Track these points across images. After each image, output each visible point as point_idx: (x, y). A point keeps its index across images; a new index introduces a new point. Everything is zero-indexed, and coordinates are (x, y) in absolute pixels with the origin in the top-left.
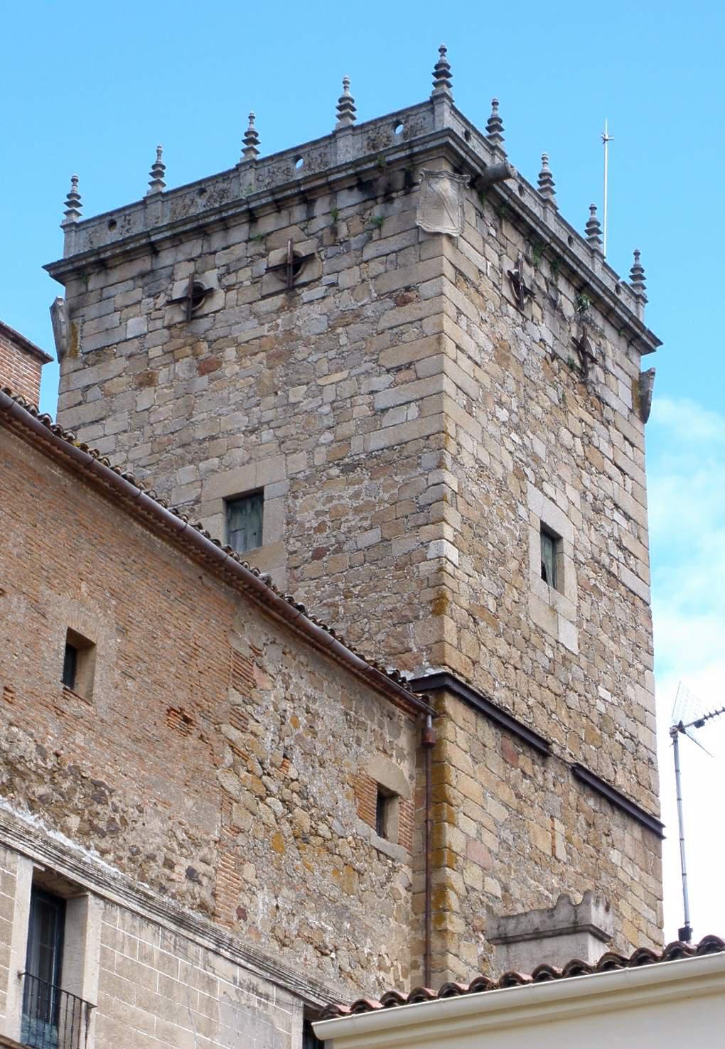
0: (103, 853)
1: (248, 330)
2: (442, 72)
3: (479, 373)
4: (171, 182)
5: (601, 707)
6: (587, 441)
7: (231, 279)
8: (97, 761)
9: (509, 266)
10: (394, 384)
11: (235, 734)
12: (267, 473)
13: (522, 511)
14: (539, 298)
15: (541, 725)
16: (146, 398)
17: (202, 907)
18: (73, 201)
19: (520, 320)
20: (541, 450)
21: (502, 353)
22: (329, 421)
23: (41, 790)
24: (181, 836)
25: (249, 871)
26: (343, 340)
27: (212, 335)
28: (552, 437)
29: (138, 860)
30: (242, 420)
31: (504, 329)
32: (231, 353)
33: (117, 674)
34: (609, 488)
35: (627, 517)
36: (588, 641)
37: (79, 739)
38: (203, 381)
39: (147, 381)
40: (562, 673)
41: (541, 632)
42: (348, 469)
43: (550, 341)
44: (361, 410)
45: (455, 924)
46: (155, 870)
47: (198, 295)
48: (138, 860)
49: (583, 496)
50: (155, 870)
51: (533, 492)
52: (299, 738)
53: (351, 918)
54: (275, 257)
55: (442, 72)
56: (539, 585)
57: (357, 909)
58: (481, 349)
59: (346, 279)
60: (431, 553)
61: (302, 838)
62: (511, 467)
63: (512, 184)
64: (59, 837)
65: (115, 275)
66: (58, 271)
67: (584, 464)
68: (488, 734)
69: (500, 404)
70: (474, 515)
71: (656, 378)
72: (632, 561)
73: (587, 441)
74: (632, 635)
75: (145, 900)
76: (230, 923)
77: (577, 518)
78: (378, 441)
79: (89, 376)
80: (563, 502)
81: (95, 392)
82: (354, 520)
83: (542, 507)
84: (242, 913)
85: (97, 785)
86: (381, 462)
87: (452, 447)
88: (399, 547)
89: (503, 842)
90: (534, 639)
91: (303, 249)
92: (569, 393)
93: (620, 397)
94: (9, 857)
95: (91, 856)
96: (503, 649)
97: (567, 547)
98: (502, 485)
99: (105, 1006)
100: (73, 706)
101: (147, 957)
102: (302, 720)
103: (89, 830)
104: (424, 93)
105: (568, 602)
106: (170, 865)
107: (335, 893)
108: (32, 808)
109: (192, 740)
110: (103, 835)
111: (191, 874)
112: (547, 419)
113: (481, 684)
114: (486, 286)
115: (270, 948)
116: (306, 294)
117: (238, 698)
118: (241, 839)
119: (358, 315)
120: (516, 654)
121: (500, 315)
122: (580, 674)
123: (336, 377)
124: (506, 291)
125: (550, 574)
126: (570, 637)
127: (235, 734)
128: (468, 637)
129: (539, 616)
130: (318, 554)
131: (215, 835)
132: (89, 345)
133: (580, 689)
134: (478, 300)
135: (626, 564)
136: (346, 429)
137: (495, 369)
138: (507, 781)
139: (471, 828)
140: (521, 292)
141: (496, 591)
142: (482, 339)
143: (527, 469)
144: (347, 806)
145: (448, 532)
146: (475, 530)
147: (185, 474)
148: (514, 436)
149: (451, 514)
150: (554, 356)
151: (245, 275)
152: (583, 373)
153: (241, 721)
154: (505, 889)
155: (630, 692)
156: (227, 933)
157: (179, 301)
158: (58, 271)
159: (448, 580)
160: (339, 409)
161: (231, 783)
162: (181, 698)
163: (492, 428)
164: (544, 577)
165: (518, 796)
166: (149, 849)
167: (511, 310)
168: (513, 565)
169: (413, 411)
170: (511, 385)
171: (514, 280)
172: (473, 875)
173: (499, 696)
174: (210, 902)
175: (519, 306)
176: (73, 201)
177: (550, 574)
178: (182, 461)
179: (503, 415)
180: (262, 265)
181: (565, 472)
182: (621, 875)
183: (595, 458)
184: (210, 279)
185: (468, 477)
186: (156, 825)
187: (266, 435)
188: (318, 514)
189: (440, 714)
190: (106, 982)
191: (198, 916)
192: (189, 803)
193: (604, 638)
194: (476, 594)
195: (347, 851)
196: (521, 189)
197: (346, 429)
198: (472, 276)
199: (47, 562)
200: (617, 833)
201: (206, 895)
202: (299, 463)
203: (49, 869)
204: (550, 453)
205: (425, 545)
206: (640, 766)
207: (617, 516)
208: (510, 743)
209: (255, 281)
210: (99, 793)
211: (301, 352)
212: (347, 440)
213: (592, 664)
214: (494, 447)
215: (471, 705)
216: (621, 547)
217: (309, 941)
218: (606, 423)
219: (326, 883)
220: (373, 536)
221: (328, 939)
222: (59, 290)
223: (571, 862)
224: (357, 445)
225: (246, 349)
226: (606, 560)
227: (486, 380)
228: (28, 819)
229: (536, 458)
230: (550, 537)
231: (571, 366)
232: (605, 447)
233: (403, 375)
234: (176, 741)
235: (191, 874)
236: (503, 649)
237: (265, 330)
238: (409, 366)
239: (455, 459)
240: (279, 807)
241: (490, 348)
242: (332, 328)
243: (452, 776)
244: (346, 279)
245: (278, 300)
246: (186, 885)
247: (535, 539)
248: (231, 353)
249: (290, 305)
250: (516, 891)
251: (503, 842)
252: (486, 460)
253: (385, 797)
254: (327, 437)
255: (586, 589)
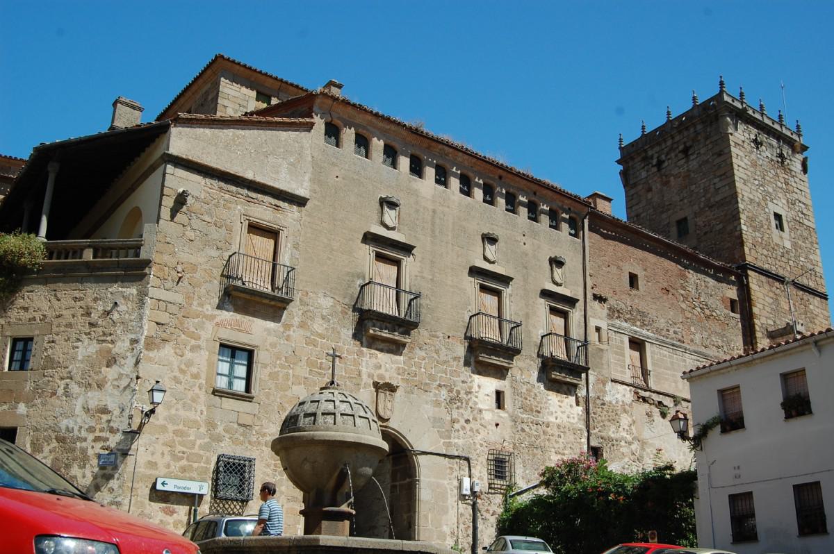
0: (648, 330)
1: (675, 171)
2: (722, 84)
3: (747, 172)
4: (648, 131)
5: (801, 263)
6: (787, 184)
7: (669, 157)
8: (643, 306)
9: (753, 137)
10: (721, 180)
11: (683, 292)
12: (687, 212)
13: (767, 210)
14: (764, 144)
15: (781, 273)
16: (650, 195)
17: (679, 341)
18: (621, 140)
19: (758, 152)
20: (771, 190)
21: (754, 165)
22: (703, 194)
23: (628, 316)
24: (670, 322)
25: (693, 329)
26: (704, 169)
27: (667, 174)
28: (775, 186)
29: (658, 331)
30: (677, 198)
31: (753, 157)
32: (672, 178)
33: (645, 282)
34: (796, 196)
35: (803, 203)
36: (795, 245)
37: (636, 301)
38: (665, 188)
39: (650, 190)
40: (786, 256)
41: (777, 245)
42: (711, 207)
43: (770, 156)
44: (712, 190)
45: (759, 335)
46: (664, 333)
47: (659, 164)
48: (658, 331)
49: (788, 202)
50: (664, 333)
51: (770, 205)
52: (703, 290)
53: (726, 337)
54: (681, 147)
55: (722, 84)
56: (776, 232)
57: (728, 335)
58: (746, 164)
59: (702, 151)
60: (738, 229)
61: (707, 317)
62: (761, 198)
63: (750, 112)
64: (635, 328)
65: (636, 160)
66: (619, 162)
67: (787, 191)
68: (763, 278)
69: (755, 179)
70: (750, 214)
71: (808, 159)
72: (807, 218)
73: (787, 184)
74: (810, 240)
75: (662, 341)
76: (689, 344)
77: (787, 208)
78: (718, 198)
79: (632, 192)
80: (780, 204)
81: (635, 196)
82: (714, 222)
83: (772, 208)
84: (692, 341)
85: (643, 313)
86: (720, 204)
87: (740, 196)
88: (730, 228)
89: (772, 309)
90: (776, 248)
91: (688, 144)
92: (778, 171)
93: (798, 167)
94: (621, 335)
95: (645, 332)
96: (765, 252)
97: (784, 218)
98: (759, 204)
99: (654, 370)
100: (634, 292)
101: (665, 356)
102: (703, 284)
103: (643, 325)
104: (717, 91)
105: (786, 234)
106: (668, 330)
107: (720, 331)
108: (626, 321)
109: (670, 296)
110: (647, 326)
111: (675, 332)
112: (772, 180)
113: (759, 264)
114: (746, 145)
115: (702, 349)
116: (692, 158)
117: (682, 282)
118: (689, 320)
119: (707, 161)
120: (770, 253)
121: (751, 152)
122: (793, 255)
123: (703, 181)
124: (753, 145)
125: (780, 227)
126: (788, 245)
127: (683, 292)
128: (753, 251)
129: (776, 240)
130: (706, 233)
131: (681, 320)
132: (632, 182)
133: (793, 259)
134: (743, 150)
135: (805, 219)
136: (709, 195)
137: (752, 169)
138: (771, 291)
139: (761, 307)
140: (757, 143)
141: (761, 236)
142: (746, 161)
143: (767, 196)
144: (721, 306)
145: (742, 222)
146: (752, 219)
147: (664, 216)
148: (761, 188)
149: (742, 216)
150: (772, 160)
151: (673, 155)
152: (782, 163)
153: (684, 288)
154: (774, 322)
155: (811, 257)
156: (688, 347)
157: (655, 165)
158: (619, 162)
159: (744, 236)
160: (706, 190)
161: (684, 306)
162: (665, 285)
163: (753, 187)
164: (777, 228)
165: (775, 294)
166: (661, 327)
167: (755, 150)
168: (766, 227)
169: (727, 187)
170: (758, 173)
171: (755, 141)
172: (763, 320)
173: (766, 267)
174: (682, 339)
175: (757, 148)
176: (621, 140)
177: (780, 227)
178: (662, 212)
179: (757, 182)
180: (677, 151)
181: (780, 195)
182: (814, 312)
183: (791, 188)
184: (663, 157)
185: (747, 204)
186: (662, 320)
187: (686, 201)
188: (704, 222)
189: (747, 276)
190: (653, 364)
191: (678, 343)
192: (671, 313)
193: (800, 242)
194: (754, 238)
195: (722, 319)
196: (754, 113)
197: (709, 195)
198: (741, 143)
199: (620, 255)
200: (811, 300)
201: (680, 337)
202: (696, 208)
203: (633, 337)
204: (774, 190)
205: (736, 227)
206: (817, 279)
207: (800, 204)
208: (771, 280)
209: (676, 156)
210: (643, 314)
211: (692, 175)
212: (709, 199)
213: (796, 250)
214: (755, 193)
215: (756, 271)
216: (803, 214)
217: (713, 345)
218: (793, 177)
219: (718, 329)
220: (721, 226)
221: (720, 344)
222: (621, 167)
223: (796, 311)
224: (712, 200)
225: (676, 176)
226: (798, 219)
227: (749, 174)
228: (625, 325)
229: (769, 193)
230: (778, 217)
231: (778, 162)
232: (794, 184)
233: (723, 177)
234: (665, 297)
235: (675, 332)
236: (765, 252)
237: (681, 170)
238: (724, 174)
239: (742, 200)
240: (699, 310)
241: (749, 163)
242: (700, 166)
243: (752, 293)
244: (702, 151)
245: (684, 161)
246: (674, 335)
247: (772, 218)
248: (672, 178)
249: (687, 162)
250: (778, 322)
251: (772, 309)
252: (752, 197)
253: (732, 302)
254: (703, 199)
255: (791, 229)
